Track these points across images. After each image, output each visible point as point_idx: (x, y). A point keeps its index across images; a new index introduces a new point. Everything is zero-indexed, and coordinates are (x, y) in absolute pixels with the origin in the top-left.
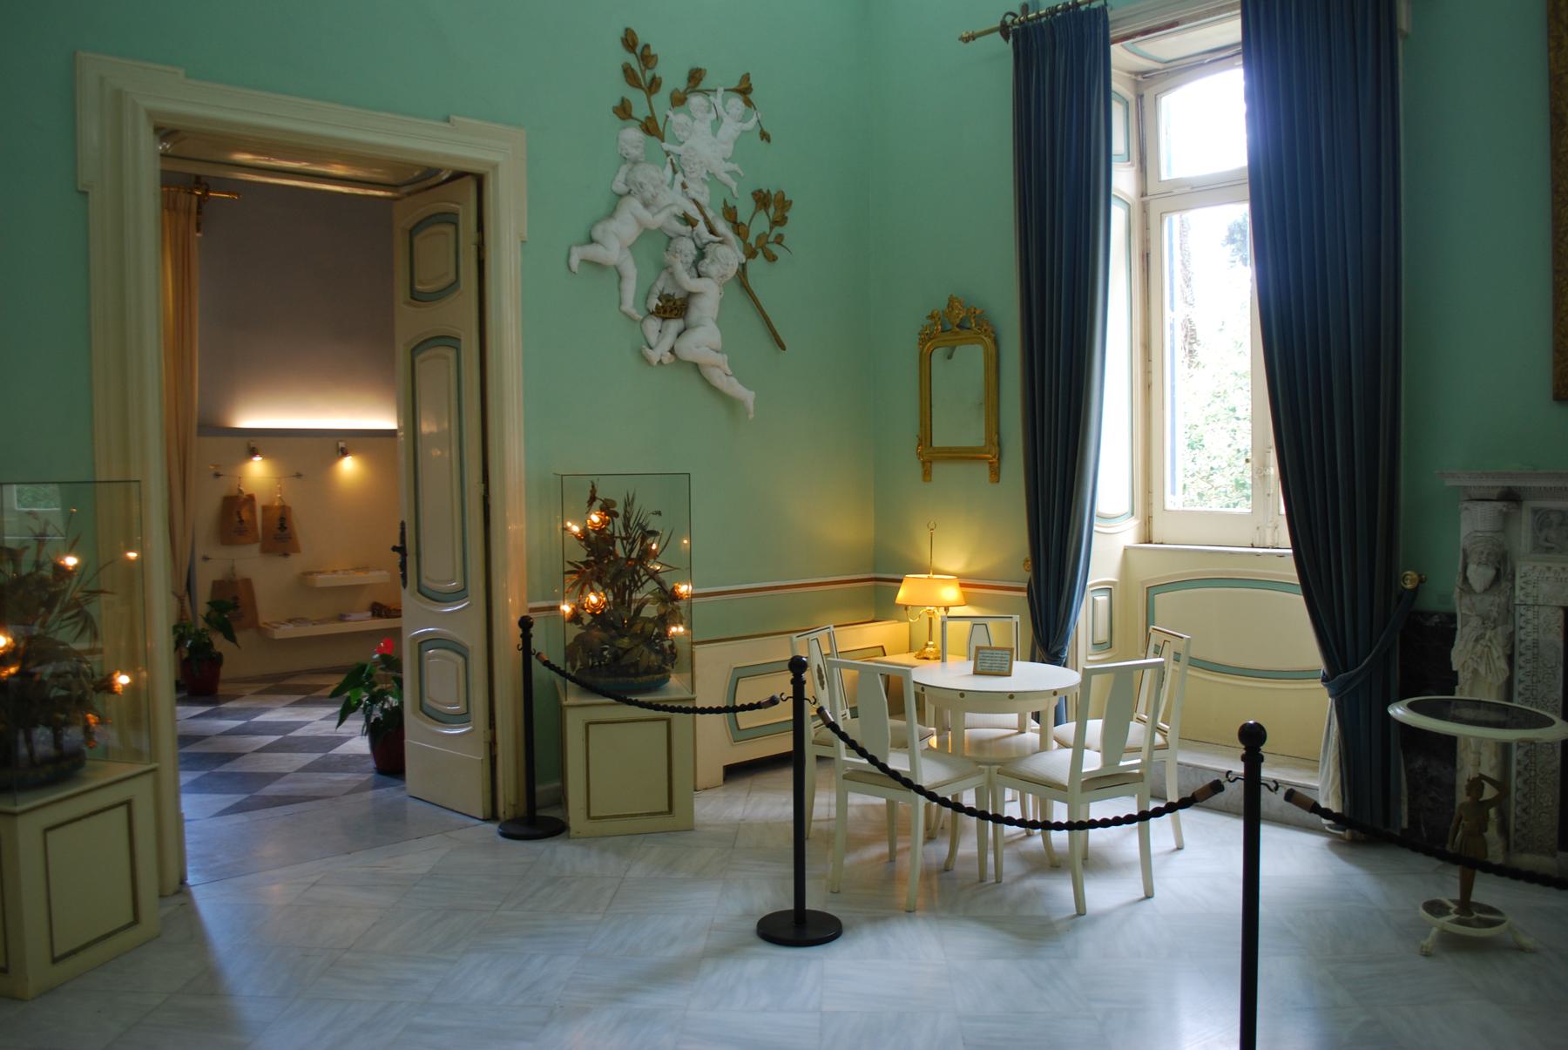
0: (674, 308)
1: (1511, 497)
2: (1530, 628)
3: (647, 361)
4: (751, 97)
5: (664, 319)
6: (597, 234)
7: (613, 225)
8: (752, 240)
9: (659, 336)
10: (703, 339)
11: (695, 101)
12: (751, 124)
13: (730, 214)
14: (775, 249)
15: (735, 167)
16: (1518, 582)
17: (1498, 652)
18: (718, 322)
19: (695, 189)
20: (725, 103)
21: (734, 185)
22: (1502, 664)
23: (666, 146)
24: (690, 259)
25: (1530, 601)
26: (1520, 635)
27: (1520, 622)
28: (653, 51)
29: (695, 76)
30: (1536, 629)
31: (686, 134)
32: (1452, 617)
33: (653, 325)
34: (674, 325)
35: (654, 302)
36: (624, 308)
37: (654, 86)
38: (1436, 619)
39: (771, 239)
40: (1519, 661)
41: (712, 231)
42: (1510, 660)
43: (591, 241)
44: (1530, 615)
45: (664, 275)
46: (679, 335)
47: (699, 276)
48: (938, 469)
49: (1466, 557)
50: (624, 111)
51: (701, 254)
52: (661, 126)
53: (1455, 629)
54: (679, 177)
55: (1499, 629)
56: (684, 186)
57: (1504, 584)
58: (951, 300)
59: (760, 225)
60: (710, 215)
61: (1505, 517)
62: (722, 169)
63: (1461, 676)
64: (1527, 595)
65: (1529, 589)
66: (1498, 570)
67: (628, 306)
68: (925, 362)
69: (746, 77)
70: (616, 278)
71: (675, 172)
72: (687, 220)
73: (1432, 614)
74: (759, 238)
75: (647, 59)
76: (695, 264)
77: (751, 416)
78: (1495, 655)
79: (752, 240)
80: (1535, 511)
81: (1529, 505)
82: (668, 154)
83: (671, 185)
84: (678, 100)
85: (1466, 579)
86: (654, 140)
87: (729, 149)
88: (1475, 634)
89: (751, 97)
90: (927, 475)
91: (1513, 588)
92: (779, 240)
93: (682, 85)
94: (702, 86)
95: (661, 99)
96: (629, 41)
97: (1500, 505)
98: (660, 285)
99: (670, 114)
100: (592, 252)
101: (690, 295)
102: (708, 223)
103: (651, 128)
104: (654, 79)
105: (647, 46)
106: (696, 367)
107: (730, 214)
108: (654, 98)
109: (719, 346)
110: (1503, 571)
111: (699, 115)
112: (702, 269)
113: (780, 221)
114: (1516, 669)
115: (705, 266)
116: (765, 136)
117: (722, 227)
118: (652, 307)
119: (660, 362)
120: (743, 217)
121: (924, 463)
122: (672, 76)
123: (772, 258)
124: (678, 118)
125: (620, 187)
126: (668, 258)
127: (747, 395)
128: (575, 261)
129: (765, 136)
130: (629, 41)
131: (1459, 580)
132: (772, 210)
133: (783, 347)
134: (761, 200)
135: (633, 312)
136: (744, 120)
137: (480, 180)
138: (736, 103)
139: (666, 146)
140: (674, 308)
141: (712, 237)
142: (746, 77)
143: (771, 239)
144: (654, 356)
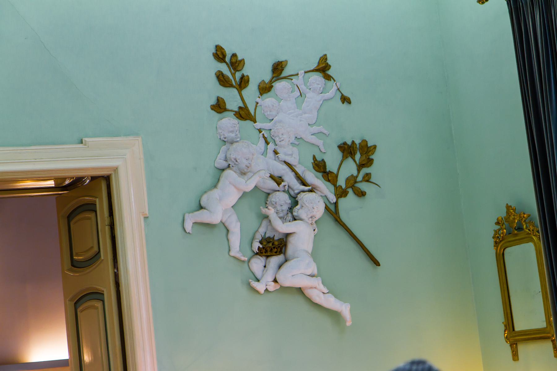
0: (274, 247)
3: (257, 292)
4: (330, 72)
5: (268, 257)
7: (215, 193)
8: (341, 182)
11: (279, 85)
12: (332, 91)
13: (320, 166)
14: (363, 186)
18: (314, 255)
23: (258, 125)
24: (286, 208)
29: (278, 69)
33: (257, 264)
34: (275, 260)
35: (257, 245)
36: (232, 253)
37: (244, 82)
39: (360, 178)
41: (304, 183)
43: (201, 207)
45: (265, 223)
46: (280, 267)
47: (295, 220)
48: (522, 349)
50: (219, 107)
51: (295, 202)
52: (252, 112)
54: (271, 146)
56: (276, 152)
58: (508, 207)
59: (349, 168)
67: (235, 251)
68: (501, 259)
69: (324, 58)
70: (225, 231)
71: (267, 143)
72: (278, 180)
74: (347, 180)
75: (236, 64)
76: (291, 209)
77: (349, 324)
79: (341, 182)
84: (265, 89)
86: (248, 123)
89: (330, 72)
90: (515, 356)
92: (367, 178)
93: (267, 76)
94: (284, 74)
95: (251, 93)
96: (219, 54)
98: (262, 230)
99: (258, 100)
100: (203, 216)
101: (287, 235)
103: (244, 114)
104: (243, 77)
105: (234, 55)
106: (300, 291)
107: (320, 166)
108: (244, 92)
109: (316, 272)
112: (295, 214)
113: (367, 162)
115: (297, 211)
116: (345, 100)
117: (312, 177)
118: (256, 250)
119: (266, 290)
120: (331, 166)
121: (511, 345)
122: (257, 71)
123: (361, 194)
125: (221, 163)
126: (264, 211)
127: (345, 309)
128: (189, 226)
129: (345, 100)
130: (219, 54)
132: (358, 156)
133: (377, 263)
134: (347, 150)
135: (239, 255)
137: (107, 179)
138: (317, 79)
139: (258, 125)
140: (274, 247)
141: (303, 188)
142: (324, 58)
143: (360, 178)
144: (260, 287)
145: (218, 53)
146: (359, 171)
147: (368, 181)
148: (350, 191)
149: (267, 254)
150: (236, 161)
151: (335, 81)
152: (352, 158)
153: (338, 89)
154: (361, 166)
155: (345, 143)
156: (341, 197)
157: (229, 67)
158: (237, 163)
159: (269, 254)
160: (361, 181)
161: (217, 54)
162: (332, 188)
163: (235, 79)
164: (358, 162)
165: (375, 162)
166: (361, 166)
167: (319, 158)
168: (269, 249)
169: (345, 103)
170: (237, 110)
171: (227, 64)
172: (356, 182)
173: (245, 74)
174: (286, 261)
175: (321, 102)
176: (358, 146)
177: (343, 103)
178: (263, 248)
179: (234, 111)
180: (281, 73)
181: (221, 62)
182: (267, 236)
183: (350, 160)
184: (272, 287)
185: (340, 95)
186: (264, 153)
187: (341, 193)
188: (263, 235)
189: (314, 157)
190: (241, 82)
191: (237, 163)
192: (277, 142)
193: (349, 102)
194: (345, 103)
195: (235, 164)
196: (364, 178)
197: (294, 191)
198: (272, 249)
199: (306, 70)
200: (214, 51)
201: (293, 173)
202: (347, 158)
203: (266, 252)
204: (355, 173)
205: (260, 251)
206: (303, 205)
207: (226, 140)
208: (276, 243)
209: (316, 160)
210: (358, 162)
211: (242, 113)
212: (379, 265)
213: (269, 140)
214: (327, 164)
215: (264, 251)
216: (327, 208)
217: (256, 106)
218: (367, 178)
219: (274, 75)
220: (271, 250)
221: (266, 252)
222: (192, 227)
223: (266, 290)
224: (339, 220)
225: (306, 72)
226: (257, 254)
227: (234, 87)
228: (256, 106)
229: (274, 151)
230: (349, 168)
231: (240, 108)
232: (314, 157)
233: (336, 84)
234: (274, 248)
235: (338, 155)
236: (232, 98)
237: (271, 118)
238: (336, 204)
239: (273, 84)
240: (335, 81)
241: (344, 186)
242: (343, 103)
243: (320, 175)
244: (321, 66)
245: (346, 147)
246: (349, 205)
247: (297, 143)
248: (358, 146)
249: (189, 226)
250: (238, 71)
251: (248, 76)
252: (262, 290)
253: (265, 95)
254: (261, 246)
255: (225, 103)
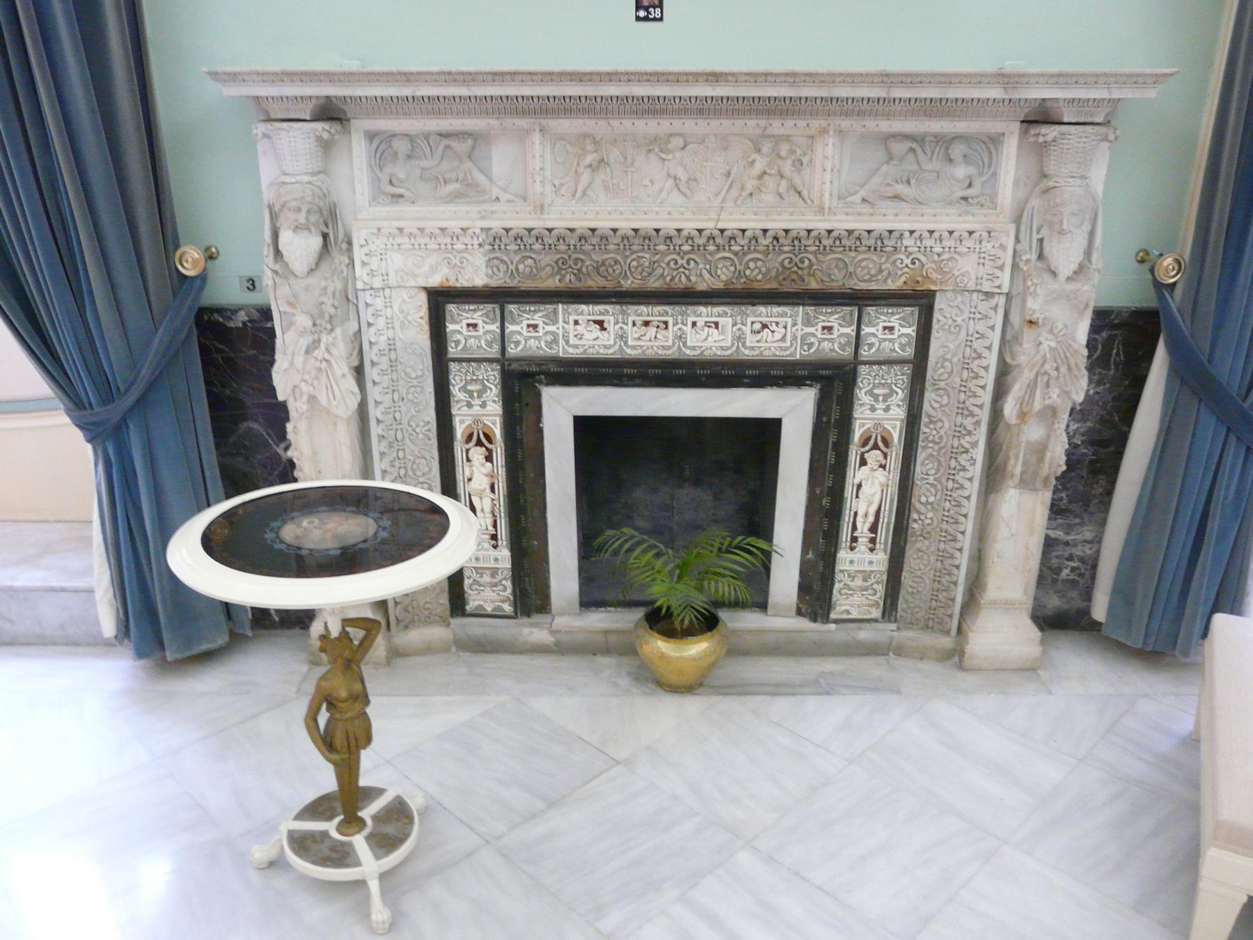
1: (330, 113)
2: (381, 323)
16: (358, 254)
17: (342, 368)
22: (350, 383)
25: (378, 283)
26: (368, 335)
27: (367, 315)
30: (390, 325)
32: (266, 313)
38: (242, 317)
40: (371, 373)
42: (359, 371)
44: (379, 303)
49: (274, 217)
53: (272, 333)
55: (338, 331)
57: (340, 259)
61: (326, 146)
63: (291, 406)
64: (372, 274)
65: (374, 263)
66: (325, 236)
73: (235, 311)
78: (339, 372)
80: (371, 136)
81: (360, 125)
85: (278, 253)
88: (304, 342)
91: (352, 263)
97: (319, 126)
110: (332, 239)
114: (369, 385)
131: (268, 252)
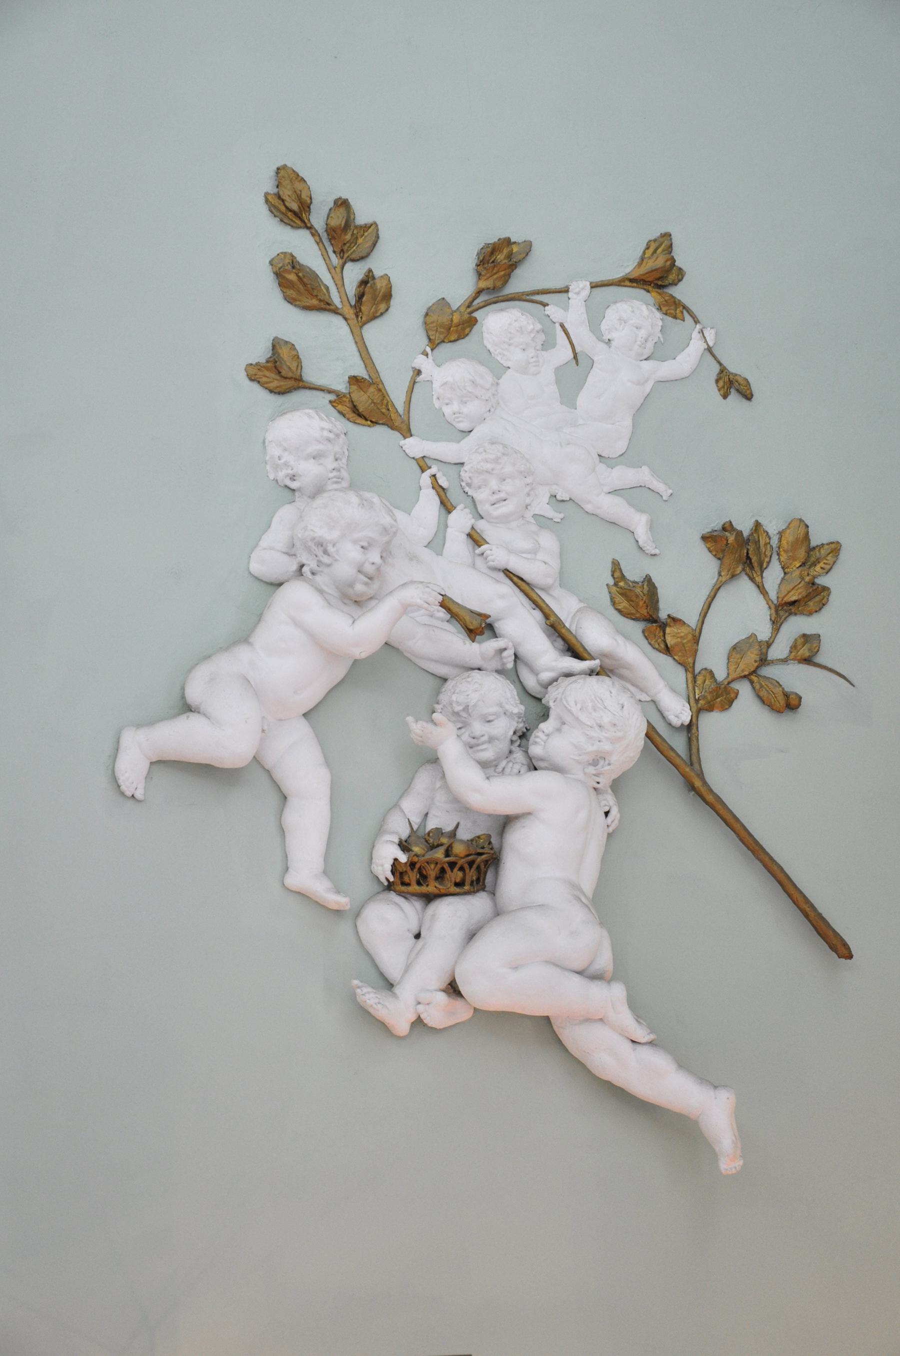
3: (383, 1027)
5: (429, 899)
6: (194, 694)
8: (714, 657)
9: (422, 950)
10: (529, 946)
11: (498, 323)
14: (793, 678)
15: (644, 475)
19: (508, 545)
20: (594, 323)
21: (640, 523)
24: (504, 728)
28: (362, 217)
29: (498, 265)
31: (473, 408)
33: (389, 920)
34: (453, 913)
35: (388, 853)
37: (372, 299)
39: (779, 650)
41: (574, 650)
43: (187, 708)
45: (424, 779)
46: (472, 935)
47: (536, 769)
50: (280, 374)
51: (537, 708)
52: (397, 397)
54: (461, 520)
56: (475, 539)
59: (743, 612)
60: (565, 607)
62: (598, 492)
67: (307, 872)
69: (664, 243)
71: (447, 506)
72: (479, 627)
75: (348, 236)
76: (523, 736)
77: (729, 1164)
79: (714, 657)
82: (423, 464)
83: (437, 543)
84: (450, 328)
86: (379, 436)
87: (617, 434)
89: (678, 292)
92: (807, 652)
93: (459, 287)
94: (521, 281)
95: (396, 339)
98: (412, 807)
99: (425, 364)
100: (185, 737)
101: (506, 822)
102: (555, 628)
103: (366, 404)
105: (343, 204)
106: (544, 1027)
107: (639, 603)
108: (373, 332)
109: (605, 961)
111: (515, 357)
112: (536, 750)
115: (548, 741)
116: (732, 385)
118: (384, 871)
119: (418, 1023)
120: (679, 599)
122: (425, 266)
124: (449, 375)
125: (268, 559)
126: (417, 728)
127: (716, 1111)
129: (732, 385)
132: (773, 576)
133: (840, 949)
134: (737, 551)
135: (321, 889)
136: (659, 352)
138: (636, 313)
139: (415, 446)
140: (453, 866)
143: (779, 650)
144: (398, 1013)
145: (286, 193)
146: (776, 624)
147: (808, 661)
148: (744, 689)
149: (423, 889)
150: (325, 552)
151: (696, 321)
152: (752, 579)
153: (709, 350)
154: (784, 609)
155: (728, 527)
156: (710, 708)
157: (320, 242)
158: (325, 559)
159: (432, 887)
160: (785, 661)
161: (279, 197)
162: (680, 676)
163: (340, 285)
164: (773, 595)
165: (834, 599)
166: (784, 609)
167: (634, 574)
168: (432, 872)
169: (734, 396)
170: (341, 386)
171: (314, 233)
172: (764, 661)
173: (377, 273)
174: (498, 913)
175: (648, 387)
176: (774, 542)
177: (725, 396)
178: (412, 865)
179: (330, 392)
180: (506, 279)
181: (295, 227)
182: (431, 825)
183: (744, 585)
184: (439, 1011)
185: (716, 369)
186: (437, 543)
187: (713, 697)
188: (416, 821)
189: (616, 567)
190: (360, 297)
191: (325, 559)
192: (483, 508)
193: (748, 396)
194: (734, 396)
195: (320, 564)
196: (794, 647)
197: (534, 672)
198: (443, 871)
199: (597, 279)
200: (269, 186)
201: (538, 614)
202: (733, 576)
203: (423, 879)
204: (764, 632)
205: (401, 874)
206: (567, 718)
207: (294, 485)
208: (459, 849)
209: (623, 577)
210: (773, 595)
211: (362, 399)
212: (850, 957)
213: (454, 496)
214: (662, 592)
215: (413, 876)
216: (651, 735)
217: (413, 383)
218: (804, 652)
219: (483, 284)
220: (441, 876)
221: (423, 879)
222: (149, 777)
223: (418, 1023)
224: (698, 784)
225: (594, 286)
226: (390, 887)
227: (336, 311)
228: (413, 383)
229: (469, 535)
230: (743, 612)
231: (354, 380)
232: (616, 567)
233: (702, 332)
234: (452, 865)
235: (705, 567)
236: (326, 347)
237: (464, 426)
238: (690, 729)
239: (475, 315)
240: (696, 321)
241: (721, 674)
242: (725, 396)
243: (636, 628)
244: (650, 265)
245: (731, 538)
246: (736, 739)
247: (557, 517)
248: (774, 542)
249: (132, 769)
250: (353, 260)
251: (386, 277)
252: (402, 1026)
253: (446, 349)
254: (403, 858)
255: (297, 357)
